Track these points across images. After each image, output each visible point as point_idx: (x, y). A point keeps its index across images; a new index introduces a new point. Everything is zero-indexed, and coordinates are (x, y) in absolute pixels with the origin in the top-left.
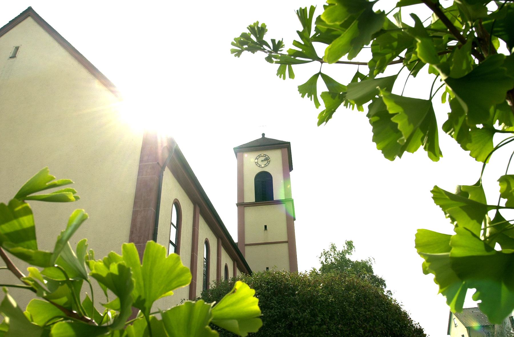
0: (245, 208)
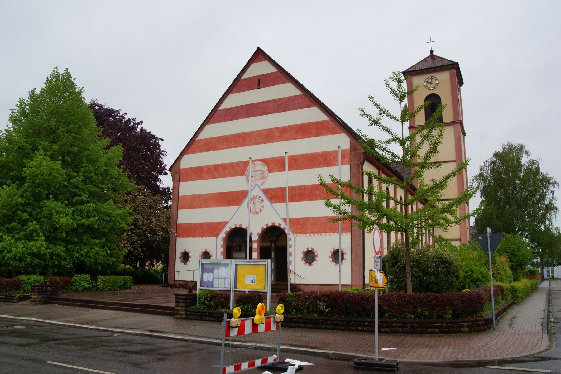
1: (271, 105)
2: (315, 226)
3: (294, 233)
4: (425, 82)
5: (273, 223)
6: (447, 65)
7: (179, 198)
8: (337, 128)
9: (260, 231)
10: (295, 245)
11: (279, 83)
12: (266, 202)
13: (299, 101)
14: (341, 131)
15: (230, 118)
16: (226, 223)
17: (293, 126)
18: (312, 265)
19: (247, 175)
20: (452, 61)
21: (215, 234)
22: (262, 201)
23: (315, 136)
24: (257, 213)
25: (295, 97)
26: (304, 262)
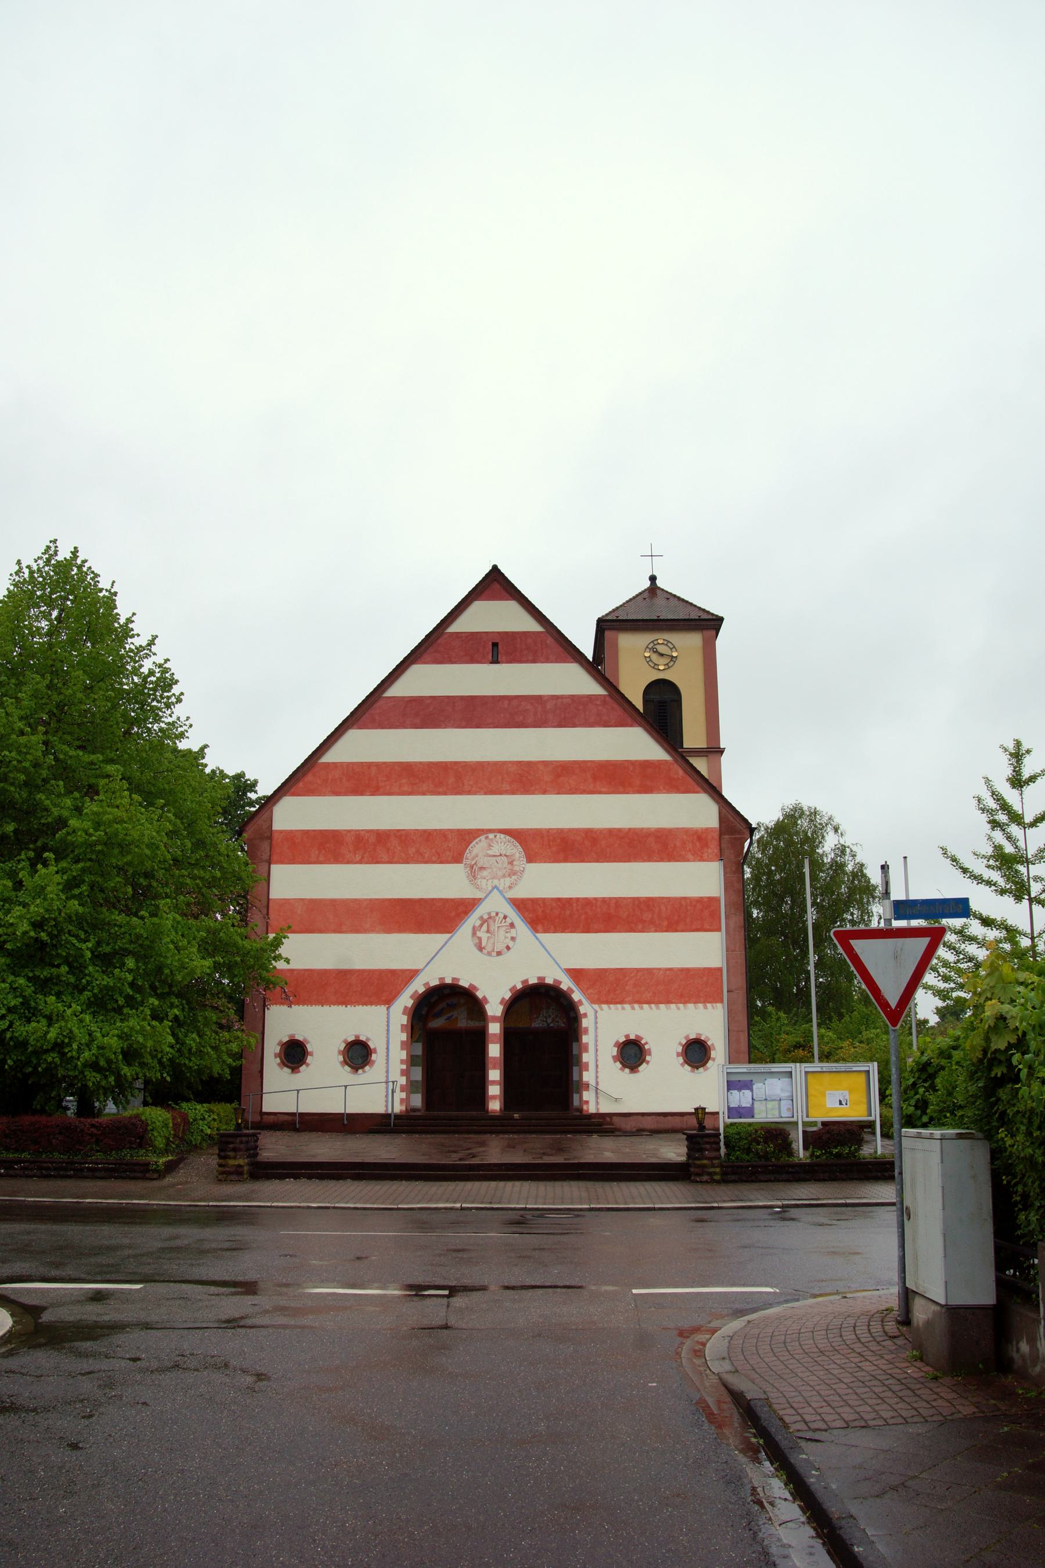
1: (529, 707)
2: (643, 988)
3: (593, 1001)
5: (539, 978)
6: (700, 620)
7: (271, 904)
8: (689, 779)
9: (508, 995)
10: (596, 1028)
11: (547, 660)
12: (522, 929)
13: (600, 708)
14: (700, 789)
15: (417, 721)
16: (413, 974)
17: (584, 762)
18: (638, 1071)
19: (468, 862)
20: (708, 612)
21: (383, 998)
22: (512, 925)
23: (639, 792)
24: (499, 953)
25: (590, 698)
26: (619, 1065)
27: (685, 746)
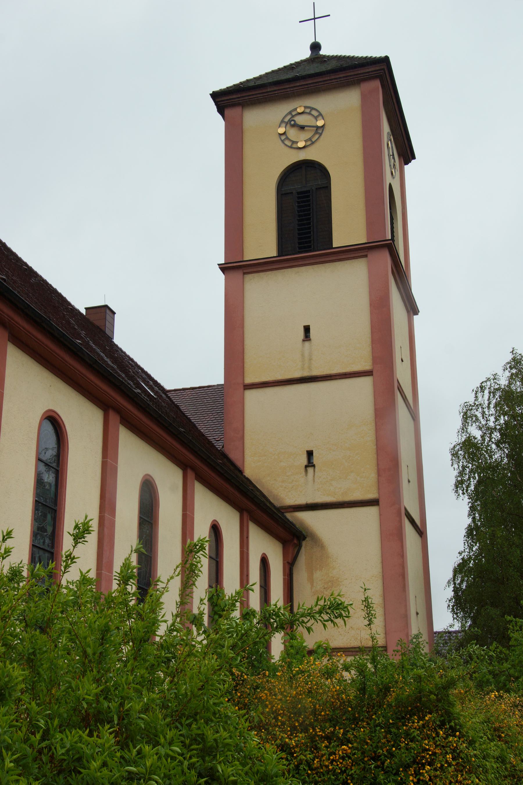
0: (248, 277)
4: (284, 125)
27: (334, 245)
